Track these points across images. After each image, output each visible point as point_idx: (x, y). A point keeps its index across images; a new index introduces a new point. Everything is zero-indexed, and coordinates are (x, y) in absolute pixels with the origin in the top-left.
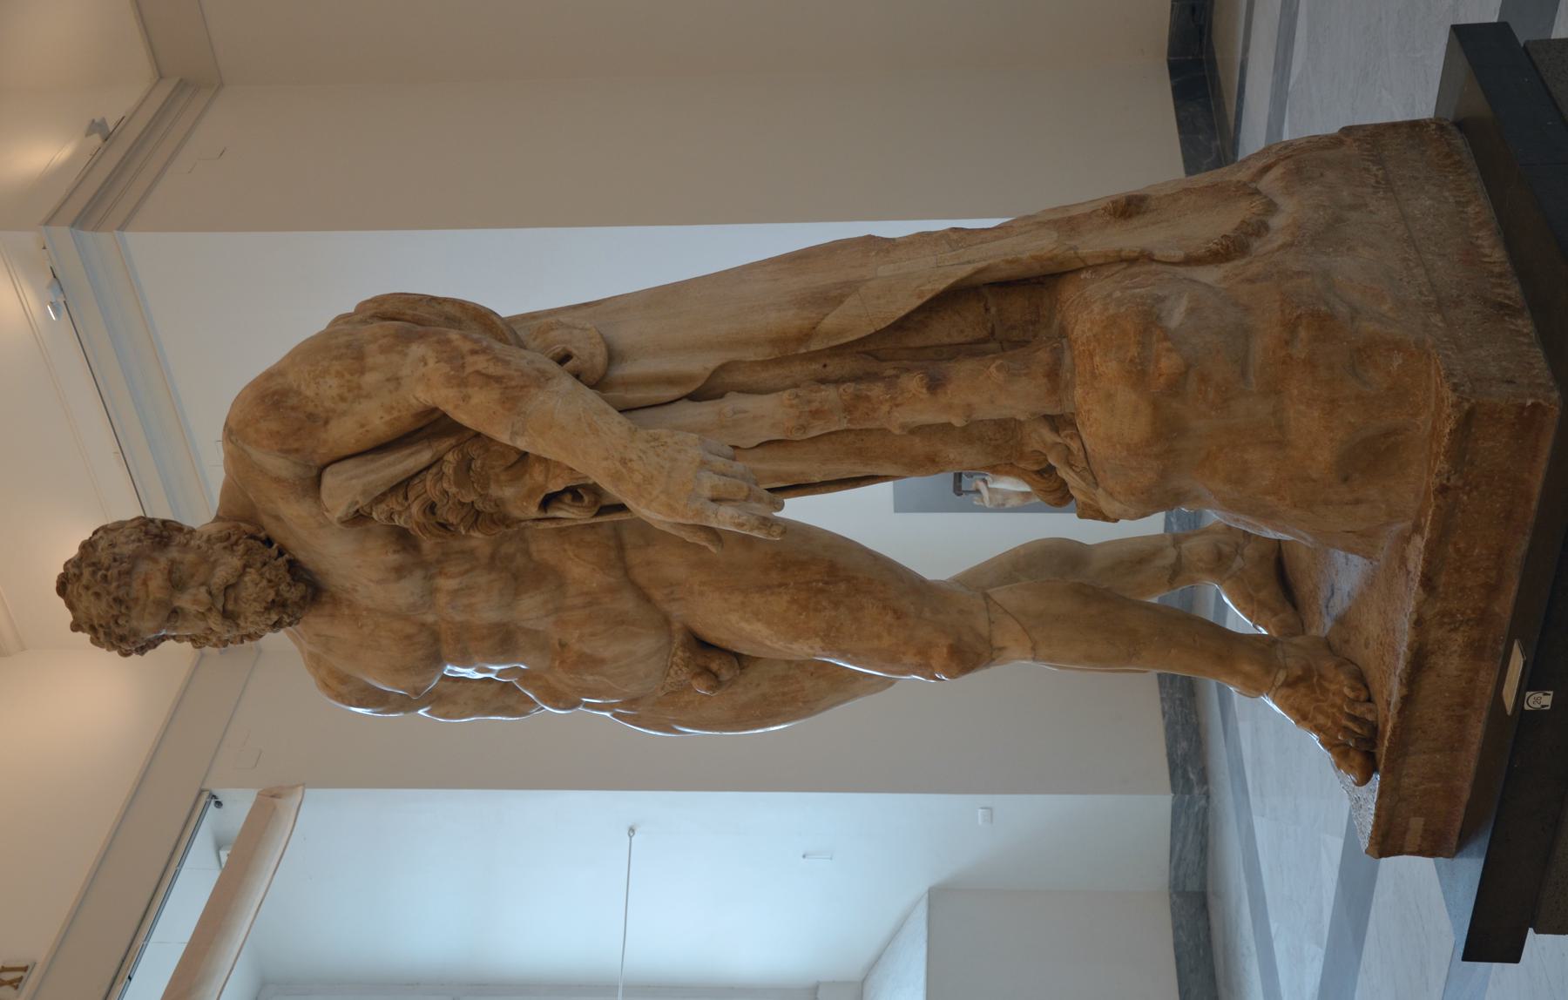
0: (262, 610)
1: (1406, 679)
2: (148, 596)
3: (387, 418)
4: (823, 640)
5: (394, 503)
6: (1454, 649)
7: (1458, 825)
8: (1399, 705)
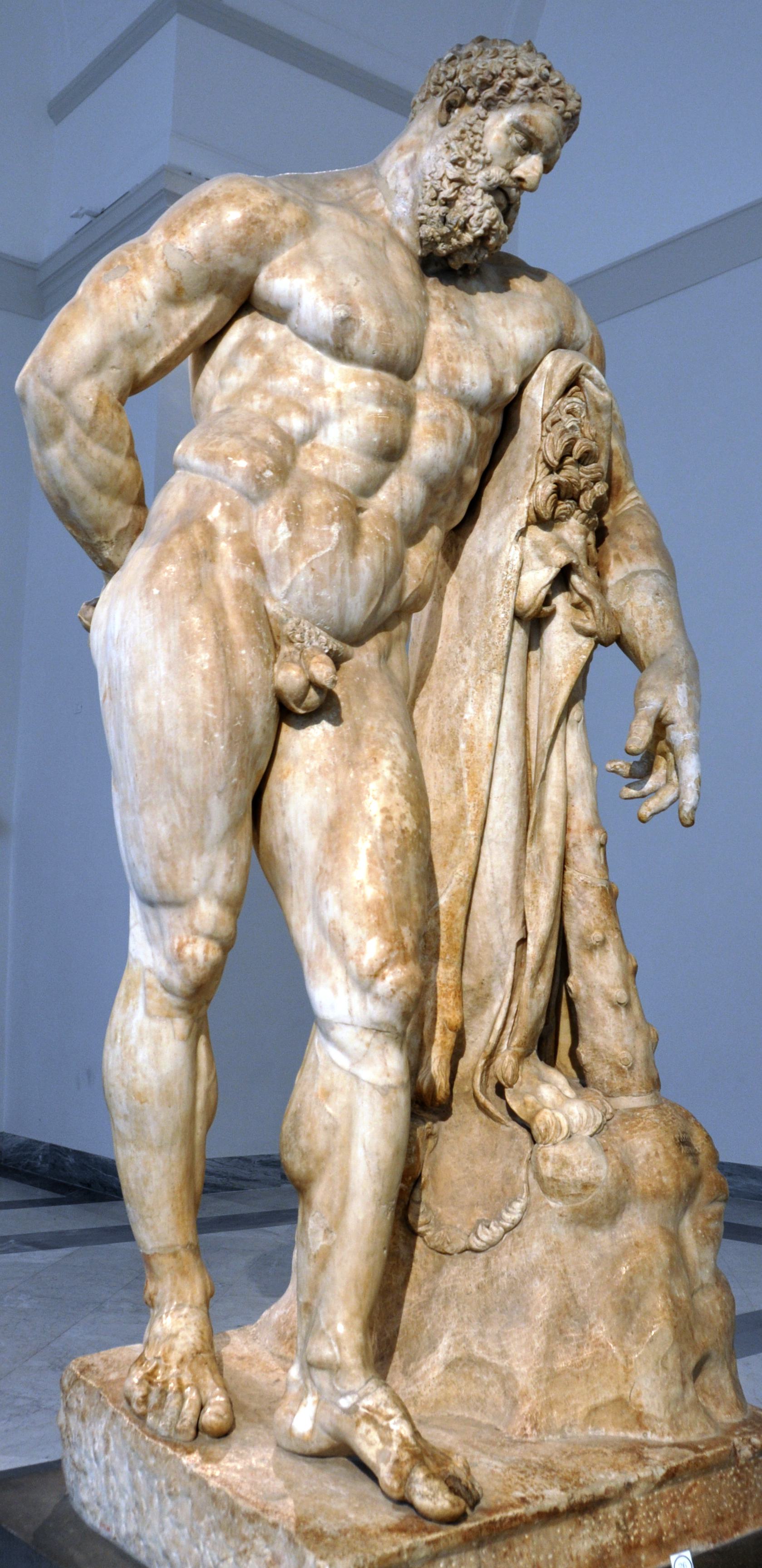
0: (495, 227)
6: (600, 1538)
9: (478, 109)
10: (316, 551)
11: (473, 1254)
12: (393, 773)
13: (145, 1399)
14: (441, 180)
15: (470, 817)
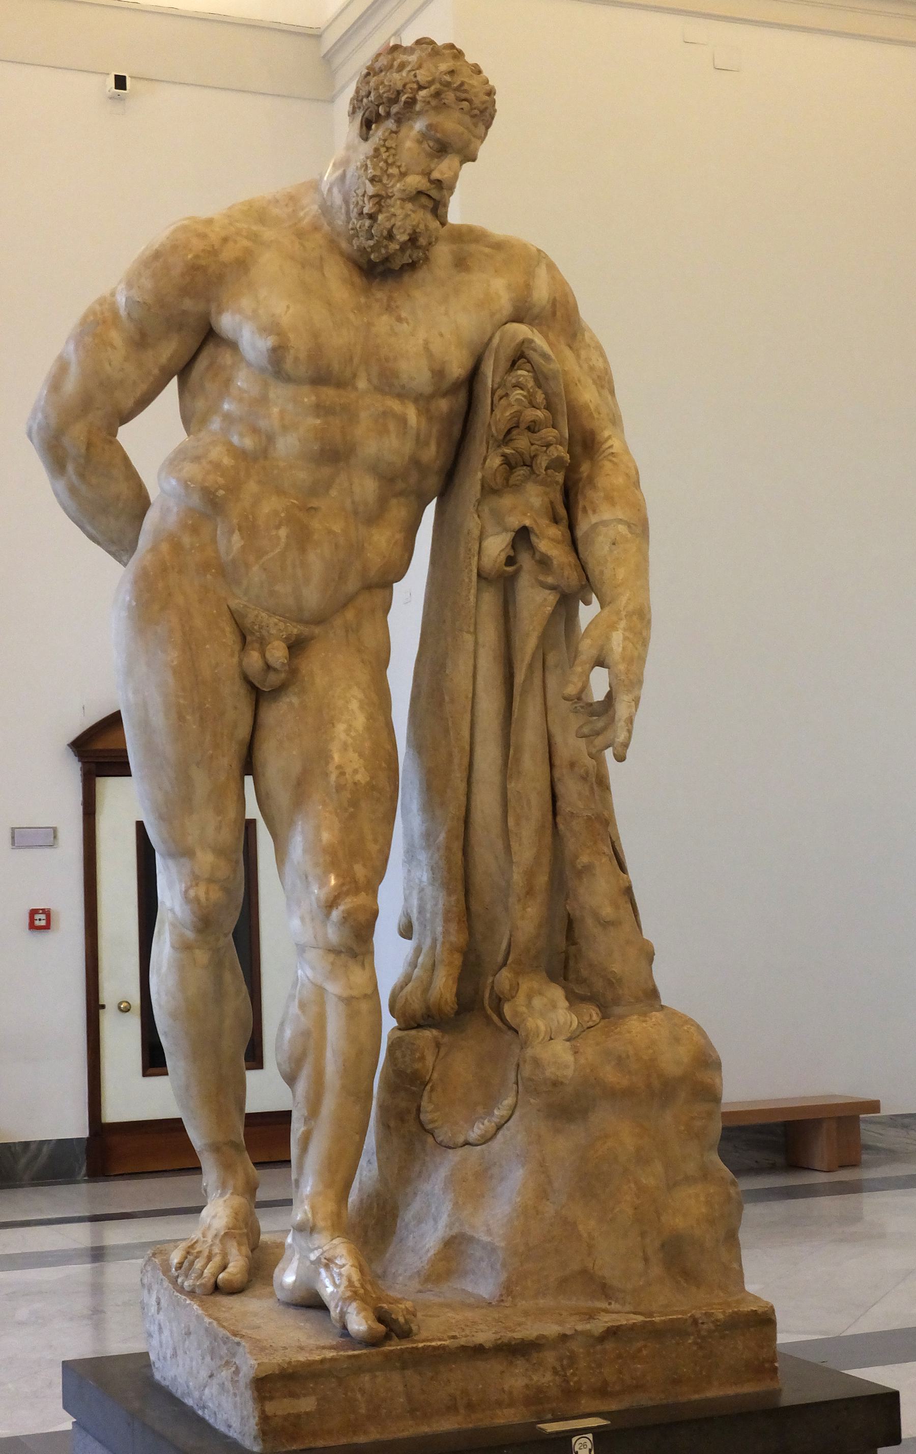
0: (418, 230)
1: (502, 1342)
2: (474, 136)
3: (592, 407)
4: (368, 783)
5: (540, 397)
6: (535, 1378)
7: (320, 1443)
8: (471, 1345)
9: (390, 124)
10: (267, 553)
11: (471, 1147)
12: (348, 735)
13: (180, 1265)
14: (363, 196)
15: (456, 761)
